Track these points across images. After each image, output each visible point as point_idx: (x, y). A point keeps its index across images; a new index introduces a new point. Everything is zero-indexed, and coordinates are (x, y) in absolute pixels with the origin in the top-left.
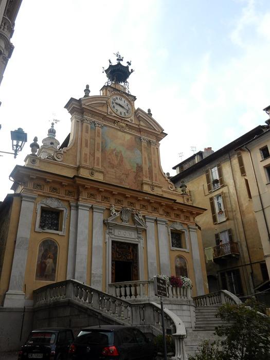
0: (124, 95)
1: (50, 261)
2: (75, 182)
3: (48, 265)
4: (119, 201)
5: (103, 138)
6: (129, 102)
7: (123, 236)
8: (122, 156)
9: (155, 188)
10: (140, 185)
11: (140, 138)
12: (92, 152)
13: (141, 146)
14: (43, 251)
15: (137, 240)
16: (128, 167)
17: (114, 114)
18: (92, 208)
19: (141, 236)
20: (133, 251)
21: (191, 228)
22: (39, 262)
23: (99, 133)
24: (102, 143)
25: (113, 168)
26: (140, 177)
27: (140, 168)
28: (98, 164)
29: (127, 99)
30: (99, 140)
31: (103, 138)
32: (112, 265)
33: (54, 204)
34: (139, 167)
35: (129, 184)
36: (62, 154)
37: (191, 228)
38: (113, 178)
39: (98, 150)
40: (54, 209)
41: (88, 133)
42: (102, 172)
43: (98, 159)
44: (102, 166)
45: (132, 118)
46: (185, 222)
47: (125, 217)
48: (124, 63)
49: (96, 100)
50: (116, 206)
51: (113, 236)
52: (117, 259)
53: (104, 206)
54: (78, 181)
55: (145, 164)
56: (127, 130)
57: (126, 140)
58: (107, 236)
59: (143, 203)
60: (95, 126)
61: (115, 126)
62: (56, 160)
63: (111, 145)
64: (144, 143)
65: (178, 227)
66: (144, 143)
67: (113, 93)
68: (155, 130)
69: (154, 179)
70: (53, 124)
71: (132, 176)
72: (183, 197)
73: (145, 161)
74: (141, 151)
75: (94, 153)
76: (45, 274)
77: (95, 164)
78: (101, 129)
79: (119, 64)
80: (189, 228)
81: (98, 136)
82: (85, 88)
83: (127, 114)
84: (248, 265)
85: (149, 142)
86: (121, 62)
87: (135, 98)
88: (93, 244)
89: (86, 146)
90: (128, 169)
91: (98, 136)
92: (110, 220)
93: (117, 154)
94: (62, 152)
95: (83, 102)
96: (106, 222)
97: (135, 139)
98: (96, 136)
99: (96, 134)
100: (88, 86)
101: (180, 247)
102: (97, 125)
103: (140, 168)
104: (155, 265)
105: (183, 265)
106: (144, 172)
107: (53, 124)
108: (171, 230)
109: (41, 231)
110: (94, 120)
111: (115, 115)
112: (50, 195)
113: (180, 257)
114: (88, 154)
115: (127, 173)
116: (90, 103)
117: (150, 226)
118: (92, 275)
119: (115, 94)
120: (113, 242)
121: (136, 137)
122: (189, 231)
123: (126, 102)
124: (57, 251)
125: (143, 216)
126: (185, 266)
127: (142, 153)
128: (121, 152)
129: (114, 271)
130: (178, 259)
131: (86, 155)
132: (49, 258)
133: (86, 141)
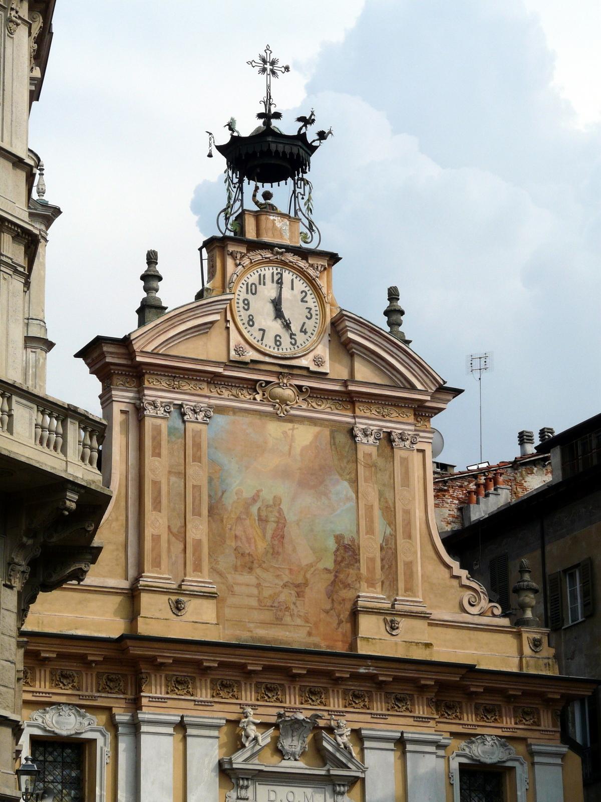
0: (290, 257)
2: (125, 650)
4: (268, 690)
5: (213, 462)
6: (311, 282)
8: (281, 522)
9: (403, 623)
11: (351, 433)
12: (179, 523)
13: (356, 461)
16: (303, 555)
17: (251, 355)
18: (181, 726)
21: (540, 754)
24: (210, 480)
25: (251, 569)
26: (347, 586)
28: (198, 568)
29: (302, 273)
34: (347, 548)
37: (540, 754)
38: (252, 608)
39: (197, 513)
40: (68, 737)
41: (159, 455)
42: (210, 596)
43: (198, 544)
44: (214, 570)
45: (323, 350)
47: (292, 744)
48: (287, 126)
50: (260, 710)
53: (221, 713)
54: (136, 650)
55: (371, 531)
56: (302, 408)
59: (354, 686)
60: (184, 422)
66: (367, 447)
67: (246, 262)
68: (413, 388)
69: (401, 585)
71: (317, 589)
72: (519, 635)
74: (354, 482)
78: (203, 427)
80: (532, 754)
81: (197, 459)
82: (144, 267)
86: (275, 123)
90: (305, 562)
91: (197, 459)
92: (239, 760)
93: (264, 514)
95: (137, 346)
96: (227, 766)
97: (333, 437)
98: (189, 459)
99: (190, 452)
100: (152, 258)
102: (190, 416)
110: (178, 398)
112: (55, 699)
115: (300, 580)
121: (335, 427)
122: (533, 764)
123: (300, 285)
125: (353, 731)
127: (357, 492)
128: (277, 501)
133: (156, 484)
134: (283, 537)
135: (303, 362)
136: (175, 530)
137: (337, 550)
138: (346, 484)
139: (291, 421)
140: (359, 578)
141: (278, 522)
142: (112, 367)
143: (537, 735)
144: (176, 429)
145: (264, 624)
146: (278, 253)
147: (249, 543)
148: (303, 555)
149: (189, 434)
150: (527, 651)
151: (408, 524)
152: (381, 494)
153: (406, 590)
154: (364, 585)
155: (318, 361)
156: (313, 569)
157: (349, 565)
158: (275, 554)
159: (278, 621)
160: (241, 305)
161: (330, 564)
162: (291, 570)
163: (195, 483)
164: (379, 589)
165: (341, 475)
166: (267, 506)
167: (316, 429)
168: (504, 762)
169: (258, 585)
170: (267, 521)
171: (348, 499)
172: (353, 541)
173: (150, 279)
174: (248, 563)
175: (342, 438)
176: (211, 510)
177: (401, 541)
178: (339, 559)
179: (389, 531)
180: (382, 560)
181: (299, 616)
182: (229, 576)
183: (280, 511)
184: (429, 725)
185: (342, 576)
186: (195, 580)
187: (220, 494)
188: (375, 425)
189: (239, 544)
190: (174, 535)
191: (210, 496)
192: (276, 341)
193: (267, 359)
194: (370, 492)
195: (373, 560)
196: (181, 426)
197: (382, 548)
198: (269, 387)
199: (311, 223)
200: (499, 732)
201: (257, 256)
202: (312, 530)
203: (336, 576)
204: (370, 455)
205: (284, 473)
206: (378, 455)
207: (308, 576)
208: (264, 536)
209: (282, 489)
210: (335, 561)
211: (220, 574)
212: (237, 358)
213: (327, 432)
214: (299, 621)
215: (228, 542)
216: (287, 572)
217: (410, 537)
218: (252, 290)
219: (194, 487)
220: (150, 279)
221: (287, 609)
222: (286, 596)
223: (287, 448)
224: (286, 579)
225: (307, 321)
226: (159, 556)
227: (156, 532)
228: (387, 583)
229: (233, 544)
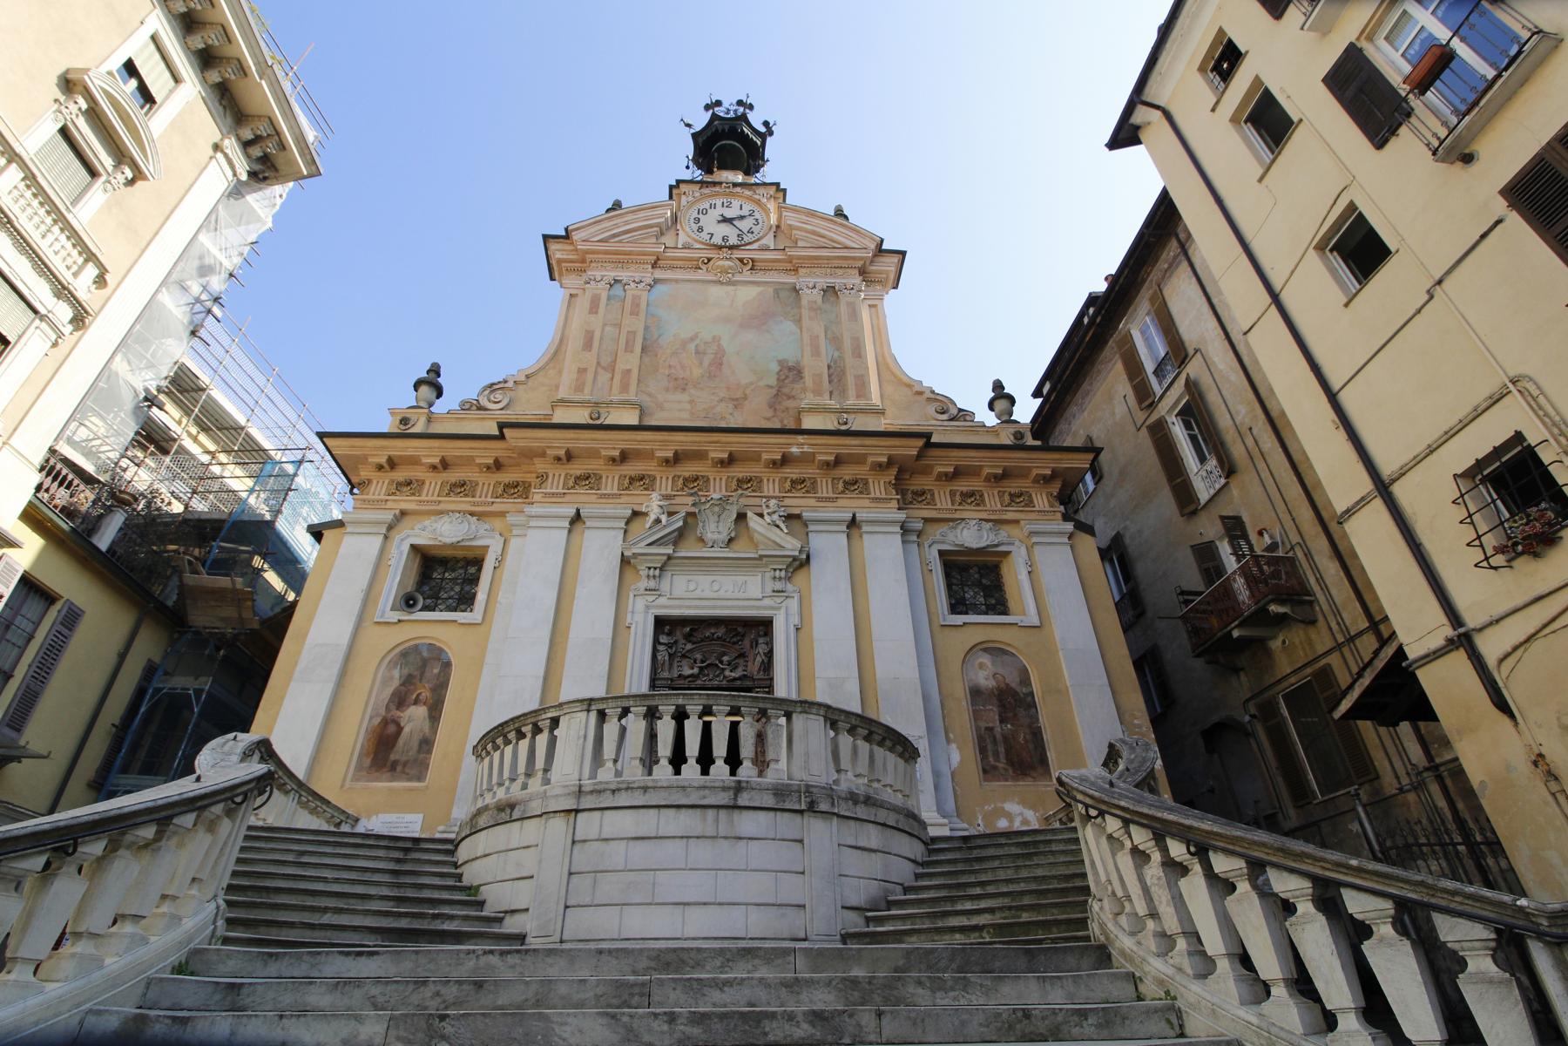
0: (738, 189)
3: (407, 730)
6: (758, 202)
11: (795, 290)
14: (396, 683)
15: (767, 602)
19: (789, 587)
22: (377, 721)
23: (638, 305)
24: (646, 328)
26: (790, 397)
29: (750, 199)
34: (790, 369)
36: (510, 389)
41: (596, 313)
46: (1009, 516)
55: (816, 352)
56: (747, 275)
60: (625, 291)
61: (701, 275)
63: (676, 327)
64: (811, 296)
65: (971, 536)
66: (811, 296)
69: (852, 392)
74: (798, 321)
76: (393, 757)
79: (714, 114)
84: (1360, 634)
89: (588, 345)
97: (777, 292)
105: (1013, 680)
106: (807, 374)
108: (941, 553)
109: (395, 616)
112: (442, 507)
113: (996, 651)
115: (739, 394)
117: (829, 547)
119: (704, 197)
124: (449, 680)
126: (1025, 680)
127: (801, 329)
128: (716, 339)
130: (985, 659)
132: (416, 702)
134: (721, 364)
136: (603, 364)
138: (789, 323)
139: (734, 285)
140: (804, 390)
142: (563, 265)
143: (1032, 516)
156: (753, 387)
157: (793, 382)
158: (711, 376)
160: (692, 221)
161: (773, 381)
162: (728, 389)
163: (630, 329)
164: (827, 396)
166: (706, 343)
167: (760, 289)
168: (997, 546)
169: (691, 402)
170: (704, 353)
172: (798, 363)
174: (681, 385)
176: (644, 349)
177: (849, 360)
178: (783, 377)
179: (836, 354)
180: (830, 376)
184: (889, 505)
185: (786, 390)
187: (656, 337)
188: (823, 282)
189: (673, 371)
191: (645, 339)
195: (820, 375)
196: (622, 293)
197: (829, 367)
198: (712, 262)
200: (984, 515)
201: (706, 191)
204: (815, 302)
207: (747, 392)
208: (701, 364)
210: (778, 379)
213: (771, 290)
217: (860, 356)
224: (722, 395)
226: (584, 384)
229: (667, 372)
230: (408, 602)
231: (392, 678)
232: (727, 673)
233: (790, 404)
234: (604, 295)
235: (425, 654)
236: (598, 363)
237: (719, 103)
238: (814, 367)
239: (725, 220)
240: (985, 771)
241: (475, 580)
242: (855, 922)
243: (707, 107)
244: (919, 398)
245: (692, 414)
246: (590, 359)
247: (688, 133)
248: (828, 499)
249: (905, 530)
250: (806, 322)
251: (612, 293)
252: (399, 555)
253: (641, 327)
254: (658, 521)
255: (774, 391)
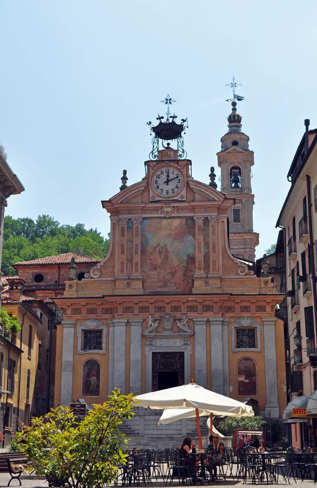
0: (172, 164)
1: (94, 378)
3: (92, 383)
5: (143, 235)
6: (179, 170)
7: (166, 345)
8: (167, 252)
10: (190, 281)
12: (130, 257)
14: (87, 371)
16: (175, 263)
20: (179, 359)
21: (265, 321)
22: (84, 381)
24: (142, 242)
25: (156, 269)
26: (191, 271)
27: (191, 259)
28: (137, 271)
29: (176, 168)
30: (138, 241)
31: (143, 235)
32: (153, 376)
33: (92, 325)
34: (191, 258)
35: (176, 284)
37: (265, 321)
39: (136, 253)
41: (124, 236)
44: (142, 271)
45: (184, 193)
46: (257, 315)
49: (130, 192)
51: (154, 347)
52: (160, 371)
55: (200, 251)
57: (173, 228)
58: (147, 348)
62: (92, 278)
64: (199, 223)
65: (246, 323)
66: (199, 223)
67: (156, 168)
68: (215, 200)
69: (211, 268)
70: (234, 104)
71: (180, 274)
73: (199, 247)
74: (194, 236)
75: (132, 258)
77: (134, 271)
79: (161, 122)
83: (176, 190)
85: (206, 220)
87: (189, 162)
88: (131, 359)
89: (123, 252)
90: (175, 265)
91: (137, 235)
92: (146, 333)
93: (160, 251)
94: (99, 267)
97: (186, 221)
100: (125, 172)
101: (254, 346)
103: (191, 259)
104: (205, 372)
107: (234, 104)
109: (82, 352)
111: (159, 199)
114: (125, 263)
115: (174, 271)
116: (124, 198)
117: (200, 329)
118: (131, 389)
119: (158, 169)
120: (153, 353)
121: (187, 218)
127: (195, 239)
128: (166, 246)
129: (155, 383)
131: (122, 263)
132: (93, 376)
134: (167, 257)
135: (176, 198)
136: (129, 260)
137: (188, 259)
138: (191, 237)
140: (195, 268)
141: (165, 253)
143: (265, 315)
144: (130, 227)
145: (161, 287)
146: (167, 163)
147: (155, 261)
148: (174, 261)
149: (134, 228)
150: (263, 286)
151: (214, 247)
152: (204, 239)
153: (213, 270)
154: (197, 270)
155: (182, 197)
157: (191, 264)
159: (165, 286)
160: (154, 182)
161: (185, 264)
162: (170, 268)
164: (203, 271)
165: (189, 234)
166: (162, 248)
167: (181, 220)
169: (158, 274)
170: (162, 253)
171: (192, 242)
172: (194, 255)
173: (124, 179)
175: (190, 222)
177: (211, 253)
180: (204, 261)
181: (173, 283)
182: (148, 273)
183: (167, 249)
185: (189, 268)
186: (135, 275)
190: (129, 261)
192: (167, 192)
193: (163, 199)
194: (200, 238)
195: (200, 261)
197: (204, 257)
198: (163, 208)
199: (183, 150)
200: (249, 315)
202: (178, 254)
203: (187, 268)
204: (200, 226)
205: (169, 236)
206: (204, 225)
207: (177, 269)
208: (161, 258)
209: (168, 242)
211: (145, 272)
212: (152, 200)
213: (184, 220)
214: (173, 285)
215: (148, 261)
216: (169, 269)
217: (215, 252)
218: (158, 177)
219: (136, 245)
220: (124, 179)
221: (169, 281)
222: (168, 277)
223: (170, 227)
224: (168, 271)
225: (178, 184)
226: (123, 269)
227: (122, 261)
228: (206, 268)
229: (150, 262)
230: (85, 348)
231: (86, 369)
232: (172, 368)
233: (190, 274)
234: (126, 228)
235: (92, 362)
236: (127, 259)
237: (162, 118)
238: (200, 257)
239: (167, 182)
240: (239, 392)
241: (100, 337)
242: (190, 432)
243: (157, 119)
244: (236, 265)
245: (159, 279)
246: (124, 257)
247: (149, 128)
248: (201, 314)
249: (223, 322)
250: (197, 236)
251: (128, 225)
252: (80, 334)
253: (140, 242)
254: (151, 325)
255: (185, 269)
